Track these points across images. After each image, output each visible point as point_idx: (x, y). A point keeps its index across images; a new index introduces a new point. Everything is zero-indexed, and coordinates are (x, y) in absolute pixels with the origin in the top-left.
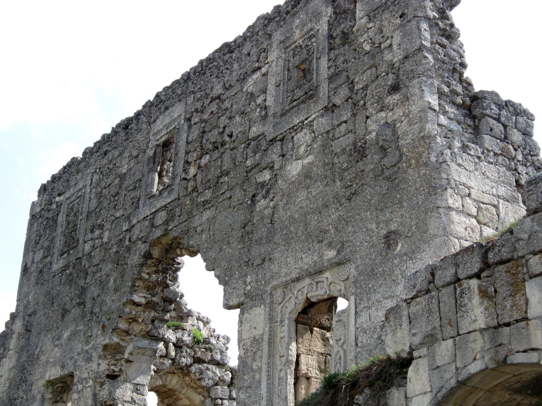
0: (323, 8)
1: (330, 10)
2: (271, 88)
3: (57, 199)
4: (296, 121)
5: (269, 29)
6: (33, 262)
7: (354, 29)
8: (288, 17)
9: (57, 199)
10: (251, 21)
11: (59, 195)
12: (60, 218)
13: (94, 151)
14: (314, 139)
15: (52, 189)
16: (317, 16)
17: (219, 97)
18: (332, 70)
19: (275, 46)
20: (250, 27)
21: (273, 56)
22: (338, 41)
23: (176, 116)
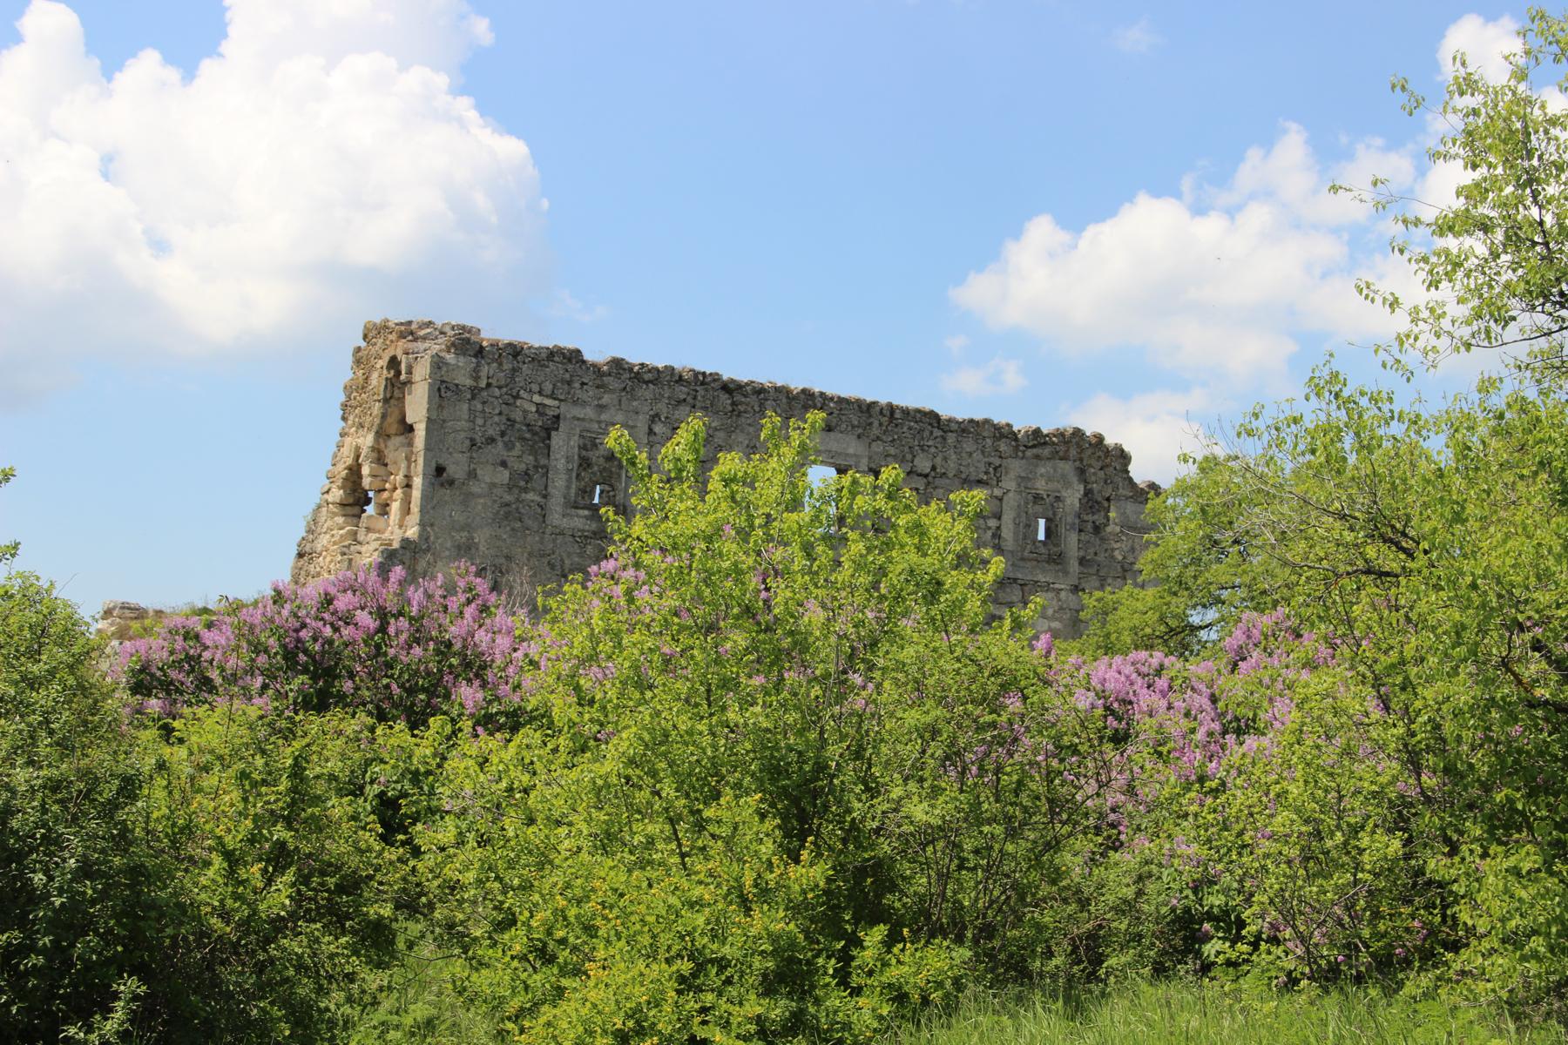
0: (1075, 480)
1: (1081, 487)
2: (1008, 517)
3: (537, 398)
4: (1041, 578)
5: (1003, 446)
6: (472, 475)
7: (1109, 529)
8: (1029, 453)
9: (537, 398)
10: (978, 417)
11: (540, 393)
12: (557, 440)
13: (647, 377)
14: (1061, 608)
15: (514, 370)
16: (1068, 485)
17: (926, 476)
18: (1082, 553)
19: (1012, 475)
20: (971, 421)
21: (1009, 483)
22: (1089, 527)
23: (851, 451)
